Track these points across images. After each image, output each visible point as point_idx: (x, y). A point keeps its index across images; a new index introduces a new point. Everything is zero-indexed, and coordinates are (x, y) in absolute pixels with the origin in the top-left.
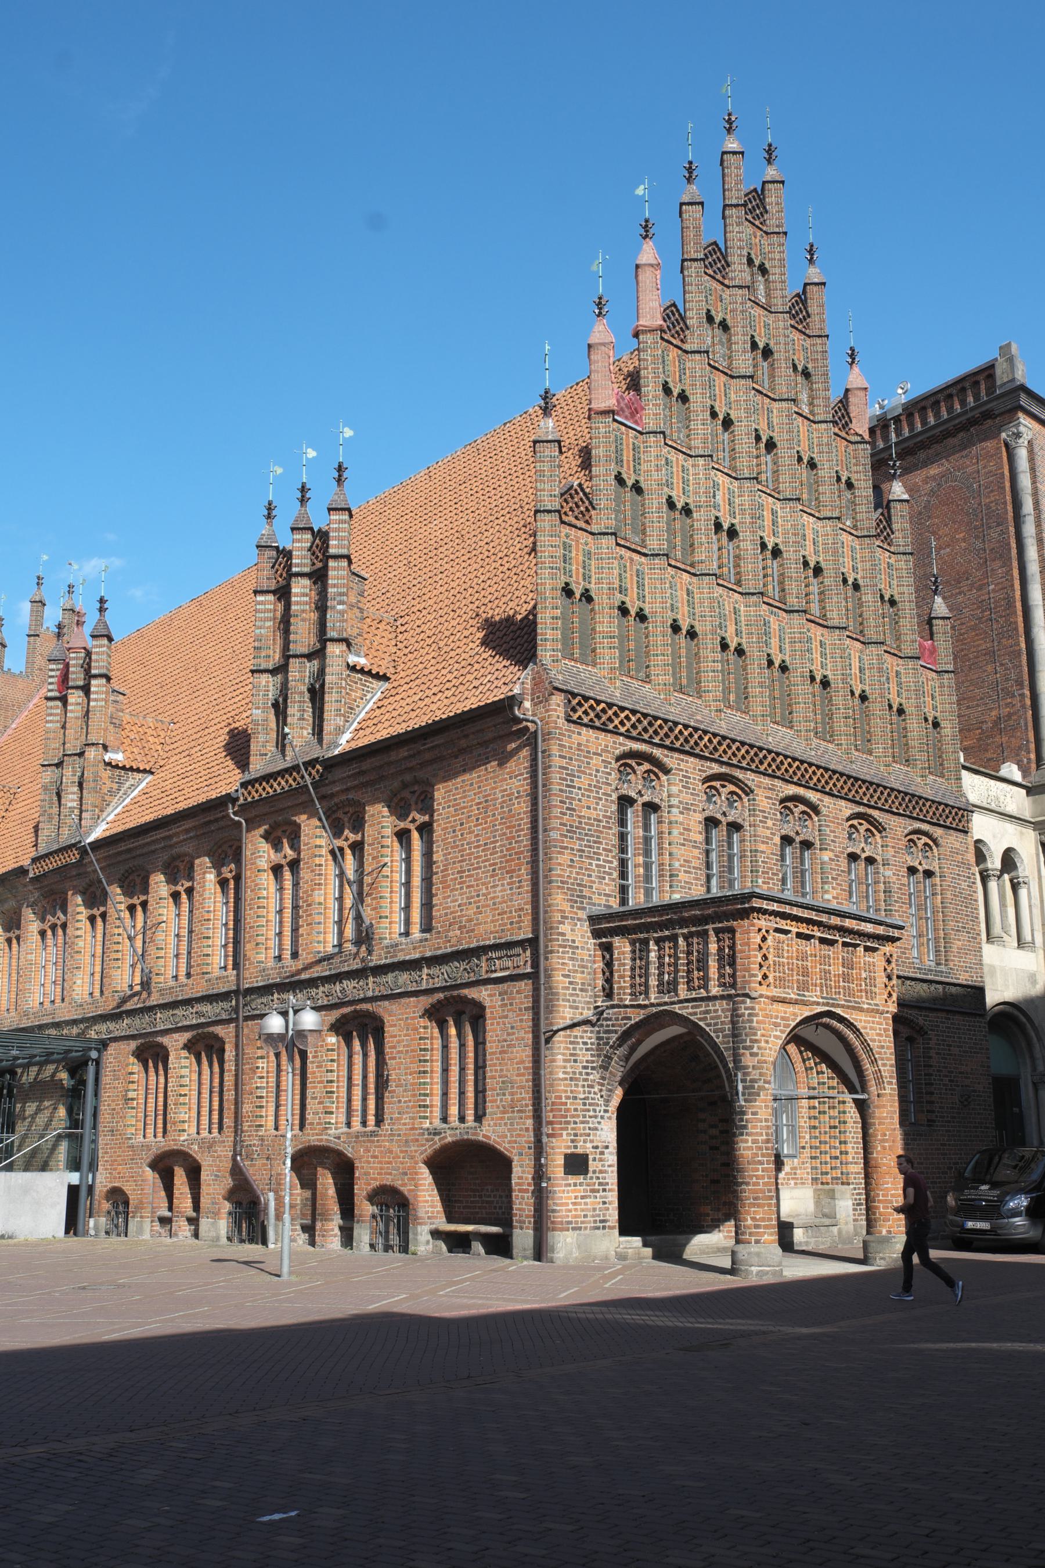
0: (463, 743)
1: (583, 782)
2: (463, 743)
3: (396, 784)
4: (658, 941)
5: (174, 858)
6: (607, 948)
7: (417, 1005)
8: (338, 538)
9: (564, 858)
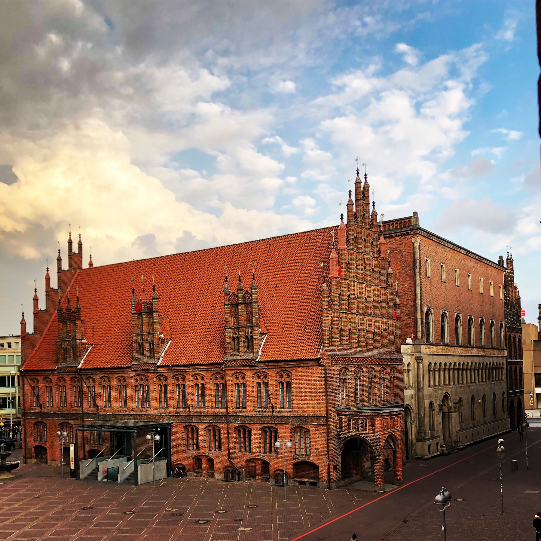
0: (302, 365)
1: (334, 379)
2: (302, 365)
3: (279, 370)
4: (355, 419)
5: (195, 374)
6: (341, 418)
7: (288, 427)
8: (255, 297)
9: (331, 398)
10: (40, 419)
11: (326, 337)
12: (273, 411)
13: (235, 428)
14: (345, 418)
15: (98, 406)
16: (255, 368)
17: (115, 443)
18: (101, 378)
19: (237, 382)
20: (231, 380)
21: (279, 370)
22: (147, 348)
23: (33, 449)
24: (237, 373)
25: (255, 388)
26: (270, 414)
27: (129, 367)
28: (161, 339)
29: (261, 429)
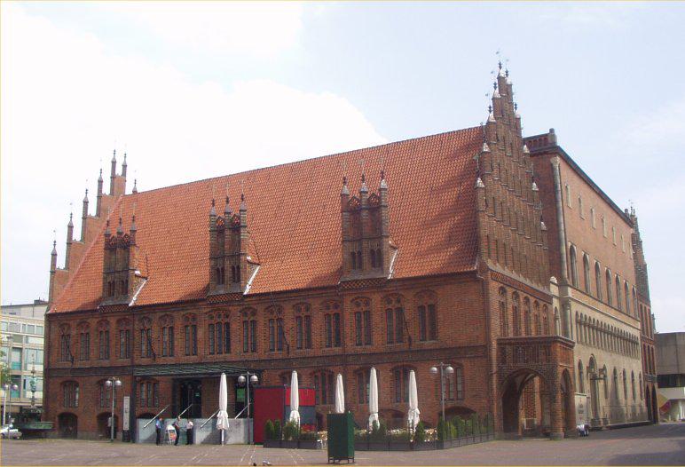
6: (503, 349)
10: (69, 376)
11: (483, 245)
12: (410, 345)
13: (355, 372)
14: (509, 349)
15: (154, 355)
16: (385, 289)
17: (178, 403)
18: (161, 318)
19: (359, 309)
20: (348, 309)
21: (418, 290)
22: (228, 274)
23: (57, 419)
24: (358, 297)
25: (384, 316)
26: (406, 348)
27: (204, 300)
28: (249, 262)
29: (392, 370)
